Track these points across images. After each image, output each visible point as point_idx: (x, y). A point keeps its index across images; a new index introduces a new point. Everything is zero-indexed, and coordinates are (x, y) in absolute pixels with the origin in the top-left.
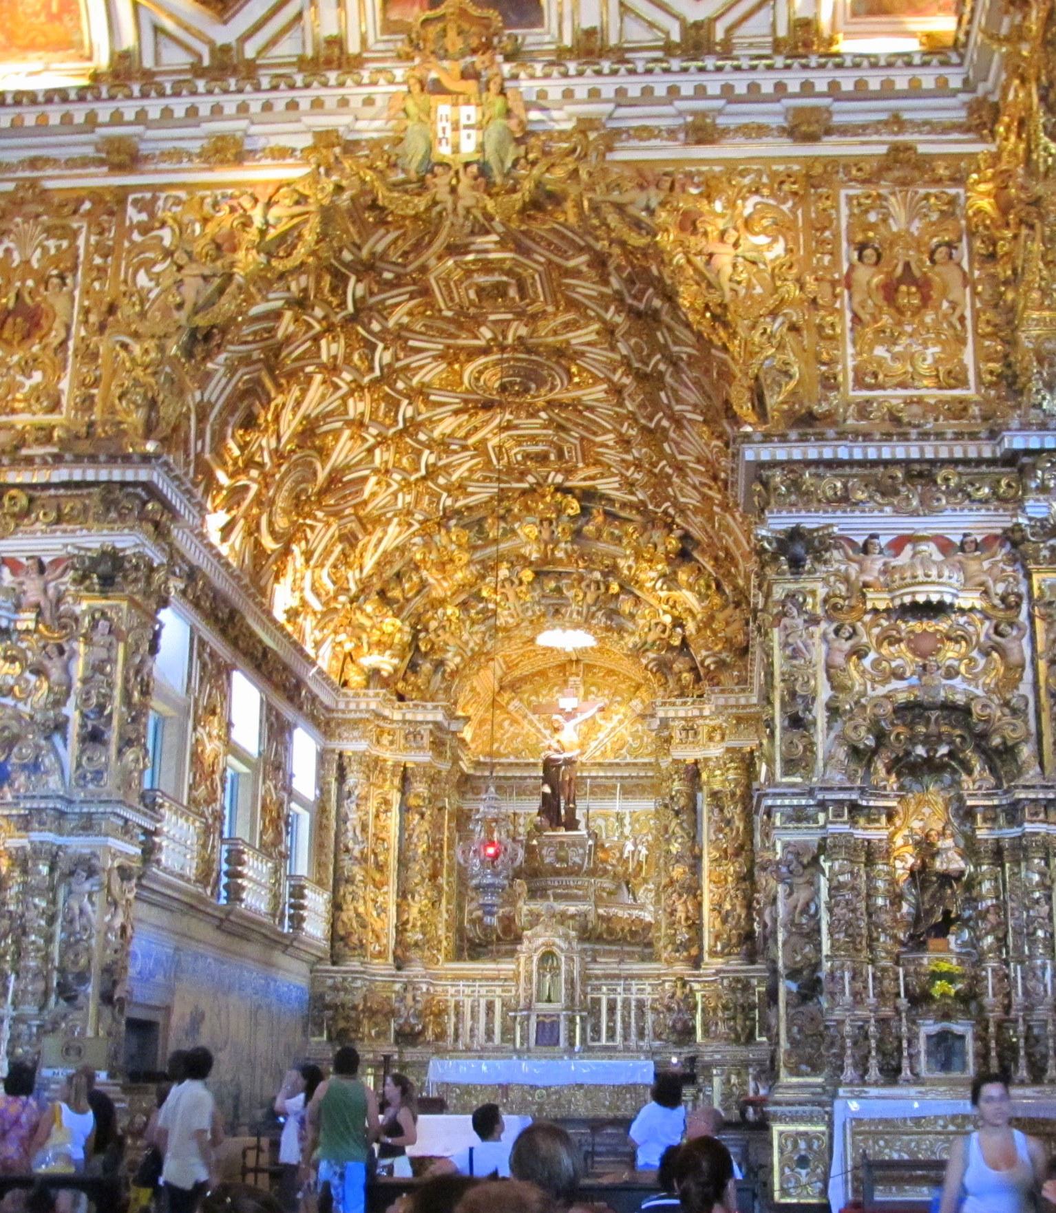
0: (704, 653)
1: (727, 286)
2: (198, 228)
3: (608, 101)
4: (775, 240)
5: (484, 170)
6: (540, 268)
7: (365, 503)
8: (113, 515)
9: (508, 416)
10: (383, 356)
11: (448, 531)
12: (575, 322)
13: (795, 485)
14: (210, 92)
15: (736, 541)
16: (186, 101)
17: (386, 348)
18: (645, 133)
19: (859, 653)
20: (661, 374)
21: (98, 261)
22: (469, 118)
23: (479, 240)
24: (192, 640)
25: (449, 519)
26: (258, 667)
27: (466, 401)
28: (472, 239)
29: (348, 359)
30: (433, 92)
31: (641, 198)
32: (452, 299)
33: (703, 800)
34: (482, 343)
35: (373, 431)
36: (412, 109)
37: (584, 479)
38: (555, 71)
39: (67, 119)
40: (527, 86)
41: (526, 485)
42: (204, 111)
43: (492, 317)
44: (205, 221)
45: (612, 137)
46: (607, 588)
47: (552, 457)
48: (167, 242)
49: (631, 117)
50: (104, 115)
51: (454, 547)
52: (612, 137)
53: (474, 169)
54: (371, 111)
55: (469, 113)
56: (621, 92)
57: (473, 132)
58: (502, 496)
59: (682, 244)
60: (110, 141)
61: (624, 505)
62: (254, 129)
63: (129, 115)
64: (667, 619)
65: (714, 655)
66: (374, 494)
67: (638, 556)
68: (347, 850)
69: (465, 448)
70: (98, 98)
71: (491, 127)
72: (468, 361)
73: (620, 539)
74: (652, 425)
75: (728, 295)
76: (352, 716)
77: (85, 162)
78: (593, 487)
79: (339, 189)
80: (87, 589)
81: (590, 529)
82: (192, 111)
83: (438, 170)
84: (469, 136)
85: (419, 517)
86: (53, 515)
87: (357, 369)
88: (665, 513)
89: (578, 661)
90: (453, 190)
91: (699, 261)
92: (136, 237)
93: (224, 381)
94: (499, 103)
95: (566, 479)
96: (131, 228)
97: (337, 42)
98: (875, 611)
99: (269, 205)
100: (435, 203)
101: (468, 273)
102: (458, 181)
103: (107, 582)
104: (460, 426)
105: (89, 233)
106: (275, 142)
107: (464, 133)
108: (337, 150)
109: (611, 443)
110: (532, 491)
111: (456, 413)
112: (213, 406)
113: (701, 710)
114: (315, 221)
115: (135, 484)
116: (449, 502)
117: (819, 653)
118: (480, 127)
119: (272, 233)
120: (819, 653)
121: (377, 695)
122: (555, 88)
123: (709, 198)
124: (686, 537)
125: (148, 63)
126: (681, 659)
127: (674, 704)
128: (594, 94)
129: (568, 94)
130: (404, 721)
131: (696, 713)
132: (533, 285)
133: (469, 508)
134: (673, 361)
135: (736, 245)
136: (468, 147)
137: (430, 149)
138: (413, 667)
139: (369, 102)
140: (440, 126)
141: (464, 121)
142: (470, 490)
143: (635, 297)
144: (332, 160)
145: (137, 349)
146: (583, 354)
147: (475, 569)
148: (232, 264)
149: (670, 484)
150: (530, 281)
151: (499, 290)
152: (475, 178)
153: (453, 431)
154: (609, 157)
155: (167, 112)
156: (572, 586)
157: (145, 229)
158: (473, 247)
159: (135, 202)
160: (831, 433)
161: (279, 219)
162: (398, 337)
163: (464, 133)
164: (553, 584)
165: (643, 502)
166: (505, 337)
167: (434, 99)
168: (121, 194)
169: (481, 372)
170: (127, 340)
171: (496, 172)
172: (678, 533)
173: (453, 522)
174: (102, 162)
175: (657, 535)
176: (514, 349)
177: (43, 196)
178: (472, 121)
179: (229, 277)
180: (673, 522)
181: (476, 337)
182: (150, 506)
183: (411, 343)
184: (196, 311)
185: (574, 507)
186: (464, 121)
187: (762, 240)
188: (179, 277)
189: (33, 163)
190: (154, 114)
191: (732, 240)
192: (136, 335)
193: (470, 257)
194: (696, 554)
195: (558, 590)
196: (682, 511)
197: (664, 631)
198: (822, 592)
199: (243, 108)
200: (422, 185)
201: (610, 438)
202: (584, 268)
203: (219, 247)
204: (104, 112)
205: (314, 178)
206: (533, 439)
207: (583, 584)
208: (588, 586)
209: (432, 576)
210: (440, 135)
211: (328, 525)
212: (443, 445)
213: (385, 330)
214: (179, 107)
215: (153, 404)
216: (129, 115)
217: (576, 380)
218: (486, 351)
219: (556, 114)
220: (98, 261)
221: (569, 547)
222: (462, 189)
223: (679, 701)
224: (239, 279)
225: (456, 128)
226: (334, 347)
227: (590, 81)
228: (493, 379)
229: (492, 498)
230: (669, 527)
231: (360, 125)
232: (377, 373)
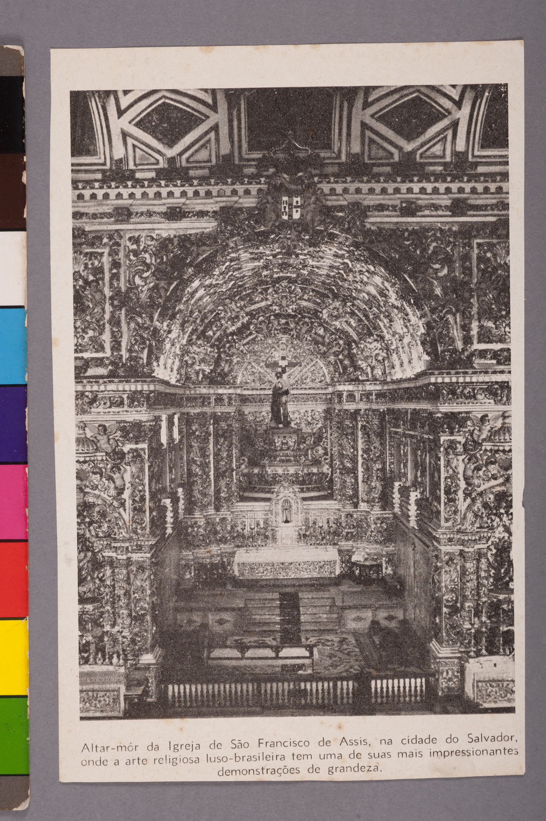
4: (443, 267)
13: (453, 392)
14: (167, 186)
16: (155, 189)
18: (381, 208)
19: (478, 469)
38: (340, 180)
39: (93, 196)
40: (326, 187)
42: (164, 194)
57: (299, 210)
62: (188, 202)
63: (125, 196)
64: (341, 342)
70: (110, 187)
82: (158, 195)
84: (297, 211)
86: (108, 404)
97: (228, 158)
98: (486, 450)
105: (110, 255)
106: (198, 208)
107: (294, 210)
117: (461, 469)
118: (302, 207)
120: (461, 469)
122: (339, 188)
125: (131, 166)
155: (145, 195)
159: (130, 239)
160: (470, 371)
174: (110, 215)
175: (337, 304)
186: (295, 204)
187: (437, 266)
190: (138, 195)
198: (463, 441)
199: (184, 194)
204: (113, 193)
208: (303, 324)
210: (283, 210)
214: (151, 192)
216: (125, 196)
220: (115, 271)
223: (347, 383)
227: (357, 185)
231: (241, 200)
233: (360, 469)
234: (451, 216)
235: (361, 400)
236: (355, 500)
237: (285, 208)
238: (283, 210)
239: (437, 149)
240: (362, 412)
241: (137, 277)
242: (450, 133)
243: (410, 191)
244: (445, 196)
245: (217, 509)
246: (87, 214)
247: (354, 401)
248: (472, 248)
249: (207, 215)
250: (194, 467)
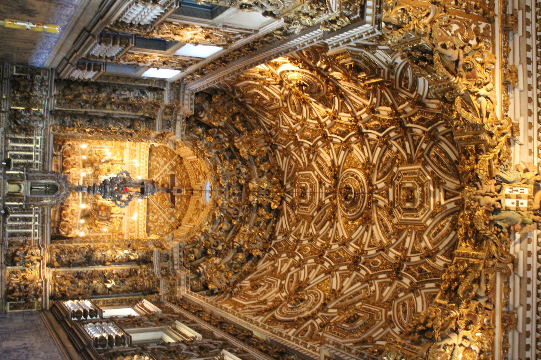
0: (205, 267)
1: (443, 343)
2: (479, 59)
3: (524, 273)
5: (497, 211)
6: (423, 222)
7: (287, 112)
9: (327, 185)
10: (373, 135)
11: (266, 146)
12: (387, 231)
15: (264, 293)
17: (378, 137)
20: (358, 270)
22: (522, 204)
23: (442, 194)
24: (251, 30)
25: (271, 147)
26: (220, 58)
27: (339, 167)
28: (442, 190)
29: (375, 118)
30: (535, 185)
31: (482, 294)
32: (405, 174)
33: (135, 266)
34: (374, 182)
35: (329, 122)
36: (528, 175)
37: (288, 212)
41: (285, 183)
43: (391, 191)
44: (482, 64)
45: (506, 276)
46: (235, 219)
47: (303, 201)
49: (515, 283)
50: (528, 15)
51: (258, 148)
52: (506, 276)
53: (499, 206)
54: (527, 152)
55: (524, 203)
56: (529, 281)
57: (515, 205)
58: (280, 172)
59: (461, 316)
61: (273, 228)
63: (528, 29)
64: (220, 248)
65: (203, 272)
66: (291, 117)
67: (250, 236)
68: (114, 91)
69: (310, 161)
71: (518, 215)
72: (365, 174)
73: (258, 225)
74: (325, 257)
75: (438, 344)
76: (181, 96)
78: (283, 214)
79: (491, 135)
81: (262, 212)
83: (498, 187)
84: (513, 203)
85: (274, 133)
87: (368, 121)
88: (270, 249)
89: (192, 193)
91: (453, 325)
92: (473, 26)
93: (384, 60)
94: (530, 220)
95: (287, 203)
96: (478, 24)
99: (487, 97)
101: (422, 185)
102: (492, 197)
104: (323, 160)
107: (515, 201)
108: (509, 135)
109: (310, 231)
110: (283, 186)
111: (333, 161)
112: (373, 53)
113: (177, 265)
114: (478, 121)
116: (279, 148)
118: (517, 209)
119: (473, 98)
121: (191, 109)
123: (482, 329)
124: (259, 258)
126: (200, 253)
127: (180, 251)
128: (529, 267)
129: (529, 254)
130: (176, 120)
131: (176, 262)
132: (413, 216)
133: (275, 156)
134: (369, 280)
136: (508, 203)
137: (508, 182)
138: (200, 124)
139: (531, 152)
140: (519, 189)
142: (285, 159)
143: (407, 270)
144: (504, 131)
145: (426, 21)
146: (367, 230)
147: (246, 157)
148: (461, 76)
149: (289, 257)
150: (415, 214)
151: (411, 199)
152: (494, 206)
153: (321, 158)
154: (498, 274)
156: (235, 202)
157: (476, 31)
158: (437, 190)
161: (480, 103)
162: (386, 144)
163: (515, 201)
164: (236, 192)
165: (275, 238)
166: (376, 193)
167: (532, 186)
168: (491, 21)
169: (357, 178)
170: (430, 17)
171: (495, 217)
172: (261, 254)
173: (269, 148)
175: (260, 244)
176: (370, 198)
178: (520, 206)
179: (455, 73)
180: (266, 252)
181: (377, 180)
182: (347, 19)
183: (379, 149)
184: (441, 54)
185: (274, 206)
186: (520, 201)
188: (457, 47)
191: (464, 343)
192: (432, 22)
193: (432, 188)
194: (250, 262)
195: (234, 194)
196: (274, 258)
197: (214, 246)
200: (491, 176)
201: (313, 230)
202: (423, 245)
203: (470, 70)
205: (498, 123)
206: (313, 193)
207: (237, 208)
208: (236, 210)
209: (246, 137)
210: (514, 189)
211: (280, 95)
212: (313, 150)
213: (390, 138)
215: (398, 27)
217: (350, 223)
218: (370, 184)
219: (518, 246)
221: (255, 202)
223: (181, 254)
224: (453, 79)
225: (518, 197)
226: (386, 113)
228: (354, 185)
229: (279, 167)
230: (265, 250)
232: (365, 130)
233: (90, 269)
235: (163, 268)
236: (56, 264)
238: (514, 189)
240: (150, 269)
245: (54, 114)
247: (160, 261)
250: (108, 90)
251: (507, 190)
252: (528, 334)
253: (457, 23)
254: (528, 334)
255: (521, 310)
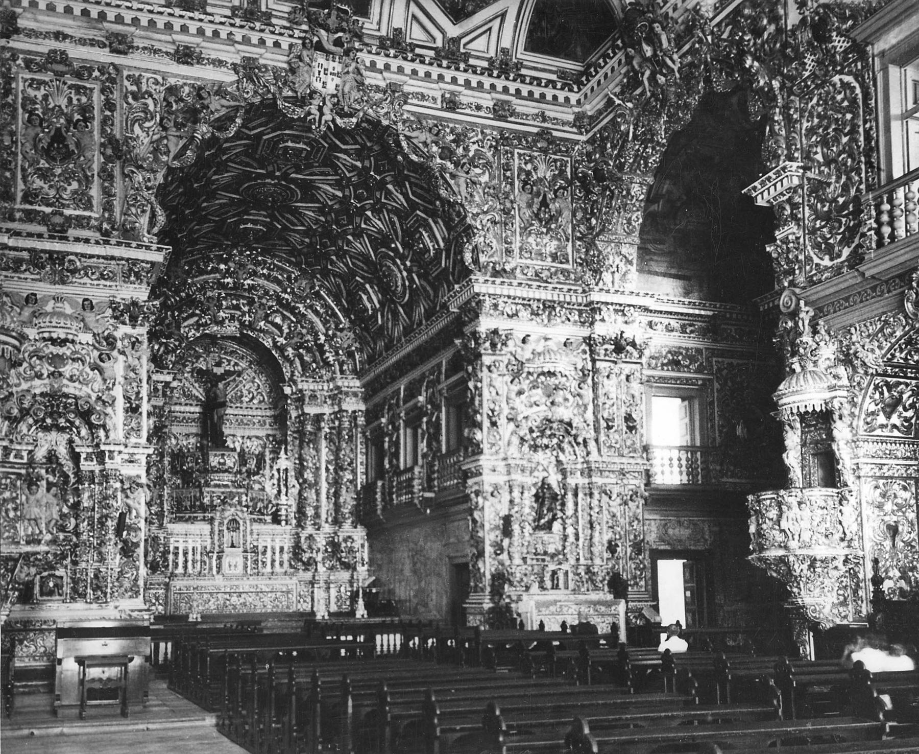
4: (484, 173)
8: (132, 278)
21: (108, 113)
22: (334, 69)
30: (316, 50)
48: (151, 107)
55: (335, 66)
57: (335, 78)
60: (116, 35)
77: (93, 43)
80: (124, 323)
84: (333, 79)
90: (320, 109)
100: (309, 113)
103: (133, 321)
105: (102, 91)
115: (147, 262)
122: (381, 62)
135: (467, 173)
136: (331, 88)
141: (331, 70)
159: (128, 77)
177: (64, 59)
178: (336, 72)
186: (331, 70)
187: (478, 171)
189: (59, 36)
222: (326, 110)
227: (399, 62)
234: (492, 119)
237: (319, 72)
238: (317, 75)
239: (479, 45)
241: (136, 126)
242: (496, 24)
243: (454, 80)
244: (488, 96)
246: (72, 37)
248: (513, 155)
249: (224, 66)
251: (318, 85)
252: (467, 83)
253: (133, 125)
254: (467, 83)
255: (442, 85)
